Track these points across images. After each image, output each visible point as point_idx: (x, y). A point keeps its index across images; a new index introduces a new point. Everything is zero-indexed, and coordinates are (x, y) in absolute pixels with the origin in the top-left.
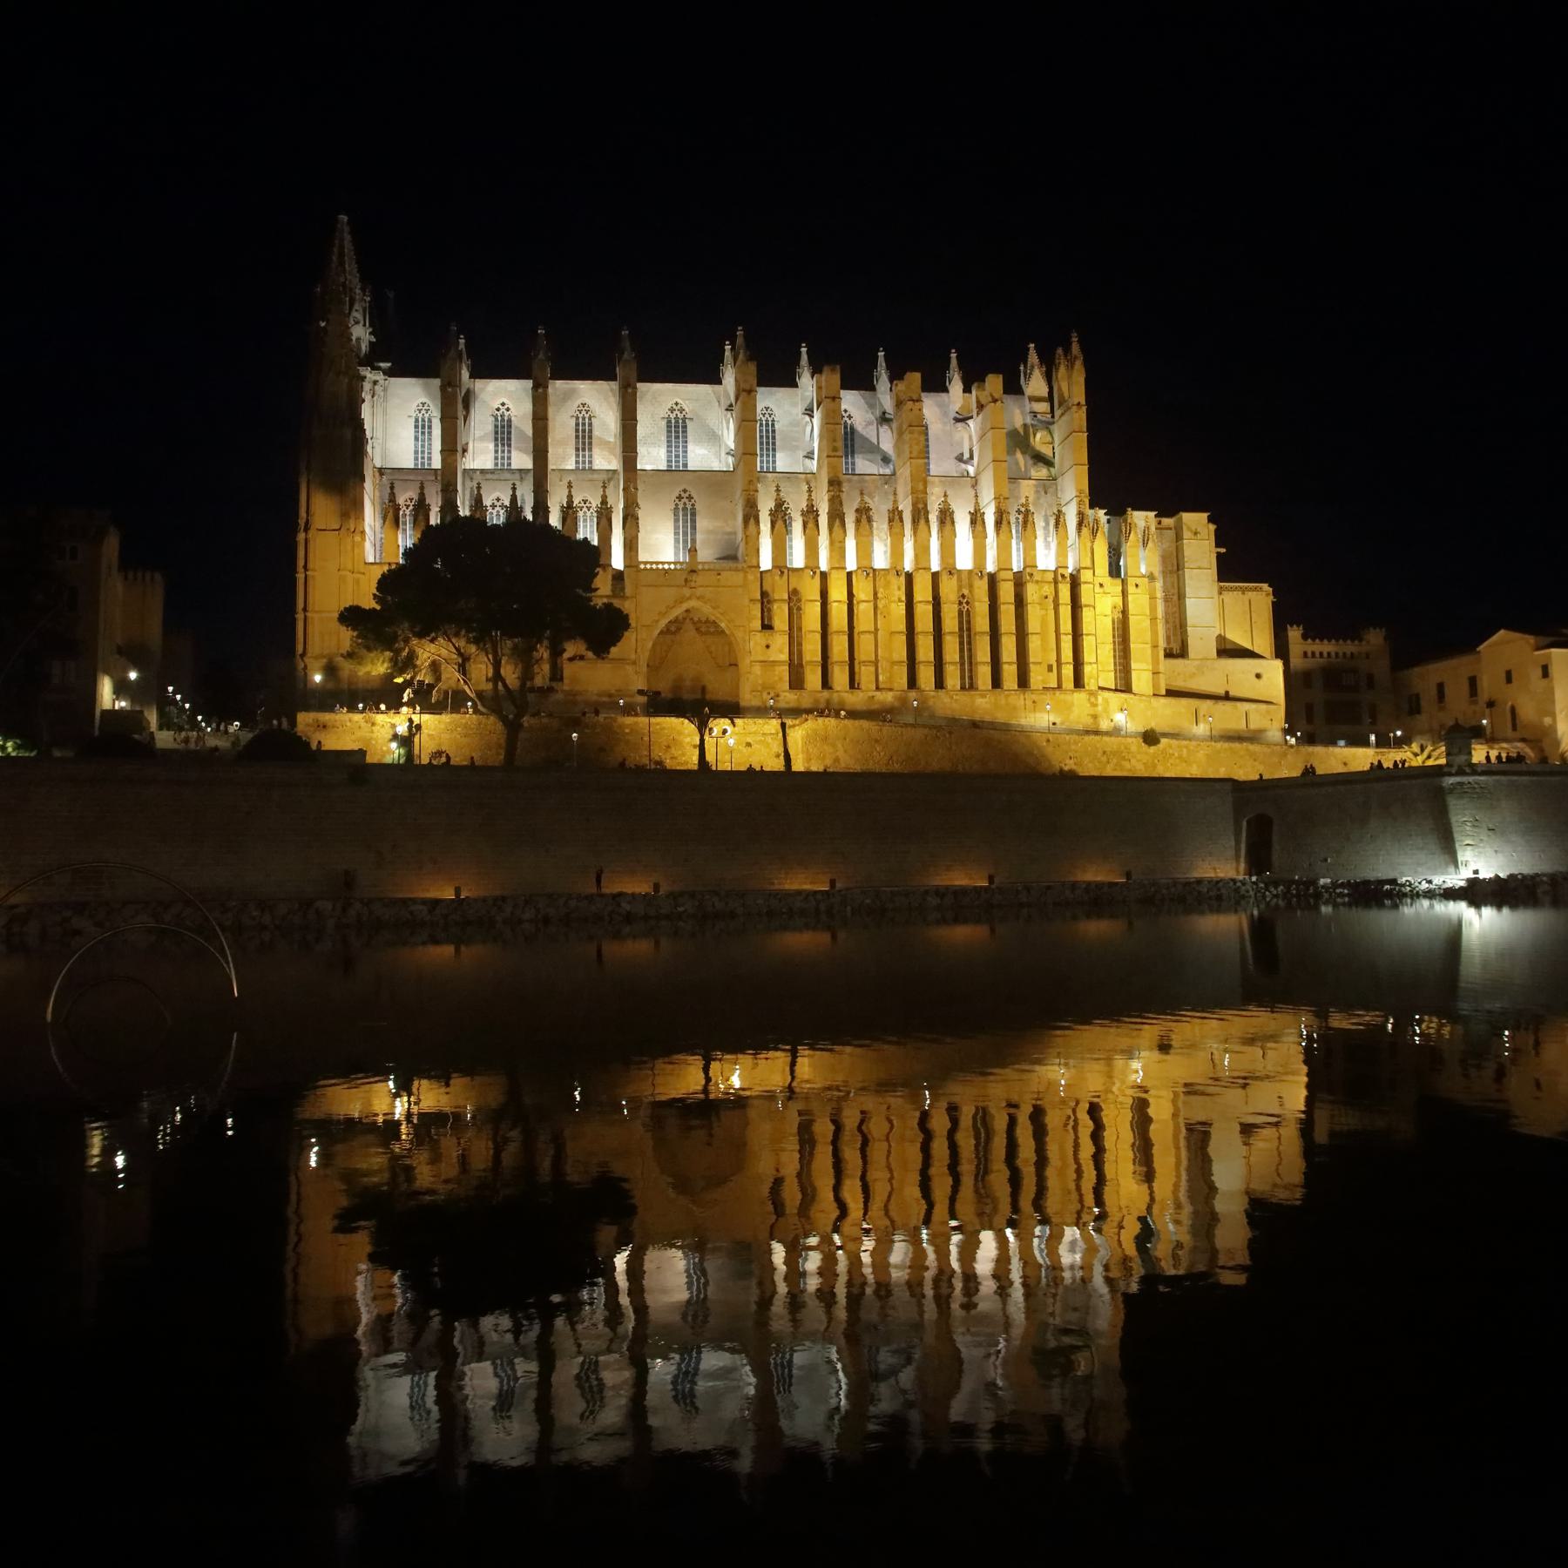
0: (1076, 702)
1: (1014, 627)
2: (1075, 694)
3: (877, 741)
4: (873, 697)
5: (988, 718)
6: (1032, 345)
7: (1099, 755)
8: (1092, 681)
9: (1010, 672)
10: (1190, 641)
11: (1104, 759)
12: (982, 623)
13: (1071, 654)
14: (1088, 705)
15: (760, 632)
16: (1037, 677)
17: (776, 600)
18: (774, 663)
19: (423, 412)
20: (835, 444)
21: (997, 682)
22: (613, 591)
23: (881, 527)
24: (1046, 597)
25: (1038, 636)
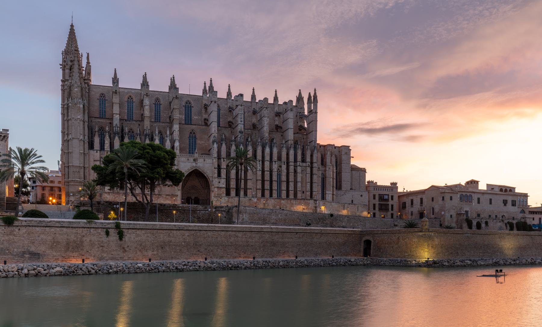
0: (310, 203)
1: (293, 180)
2: (310, 200)
7: (317, 219)
8: (316, 196)
9: (291, 193)
10: (343, 185)
12: (284, 178)
13: (310, 188)
14: (314, 204)
16: (299, 195)
17: (222, 168)
18: (221, 188)
19: (103, 97)
20: (241, 120)
21: (288, 196)
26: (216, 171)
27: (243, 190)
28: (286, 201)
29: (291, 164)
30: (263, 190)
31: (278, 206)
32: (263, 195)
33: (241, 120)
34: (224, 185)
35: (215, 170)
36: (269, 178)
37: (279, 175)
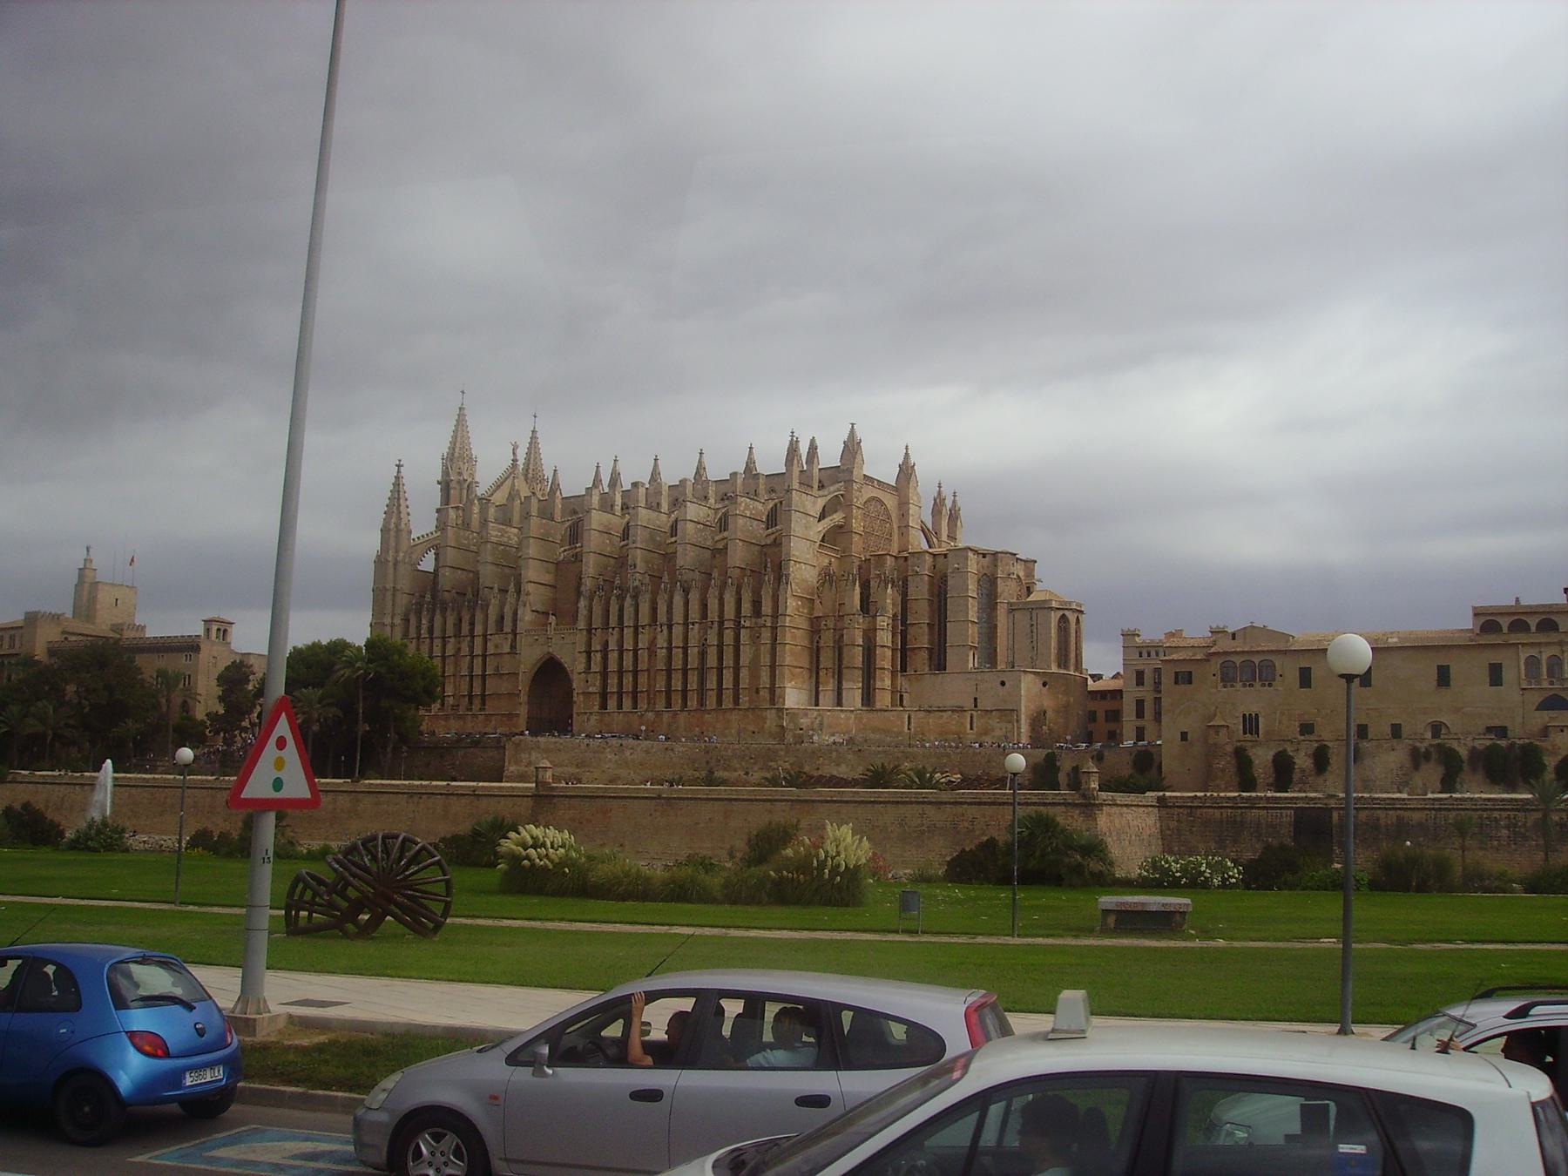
0: (769, 717)
2: (768, 711)
7: (747, 758)
11: (752, 761)
12: (712, 660)
16: (744, 699)
21: (720, 701)
22: (511, 649)
26: (583, 659)
27: (630, 695)
29: (727, 624)
30: (669, 692)
31: (697, 729)
32: (669, 705)
34: (595, 688)
35: (579, 655)
36: (680, 662)
37: (703, 655)
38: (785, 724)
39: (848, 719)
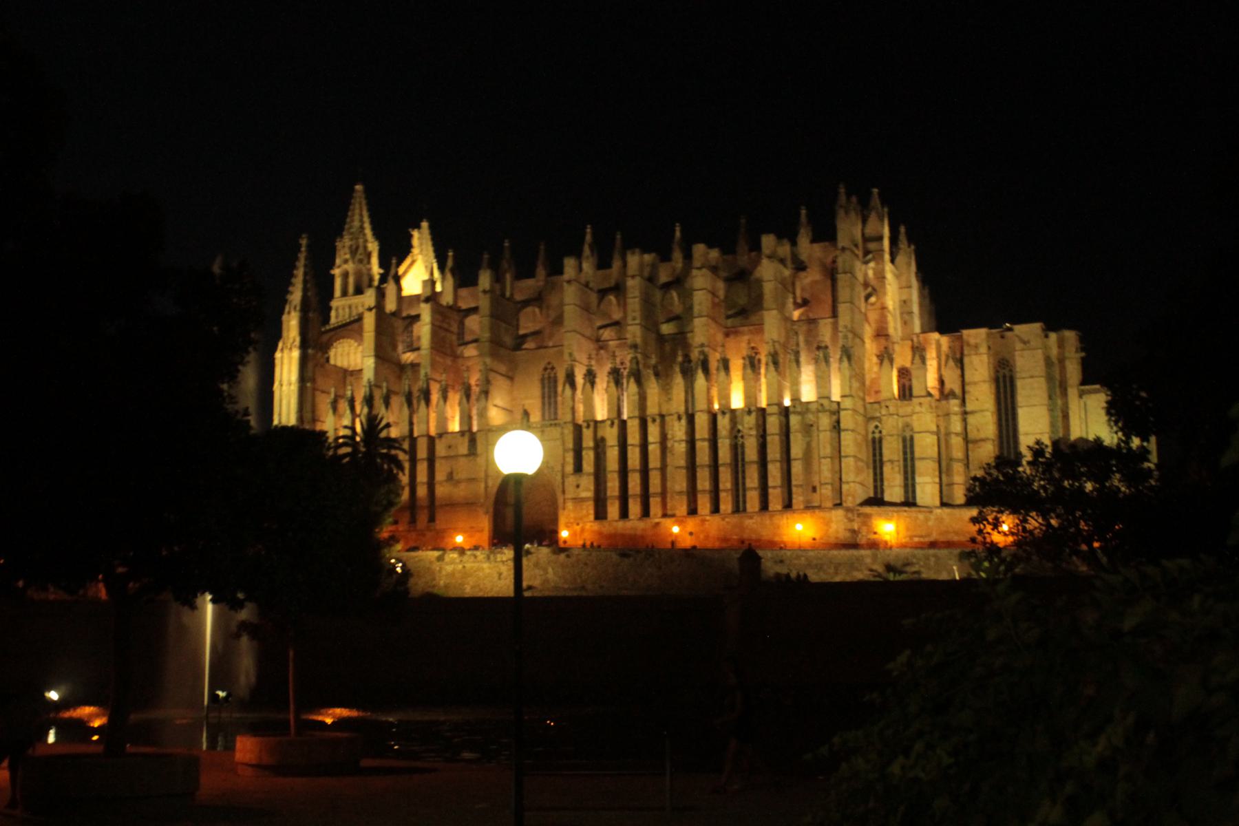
0: (834, 519)
2: (833, 512)
3: (586, 564)
4: (658, 524)
5: (754, 537)
6: (875, 191)
8: (850, 498)
12: (751, 453)
14: (846, 520)
15: (572, 474)
16: (798, 500)
18: (583, 500)
20: (634, 314)
21: (764, 506)
22: (469, 450)
23: (602, 382)
24: (812, 426)
25: (799, 462)
26: (570, 458)
28: (757, 519)
33: (634, 314)
38: (856, 527)
39: (927, 520)
